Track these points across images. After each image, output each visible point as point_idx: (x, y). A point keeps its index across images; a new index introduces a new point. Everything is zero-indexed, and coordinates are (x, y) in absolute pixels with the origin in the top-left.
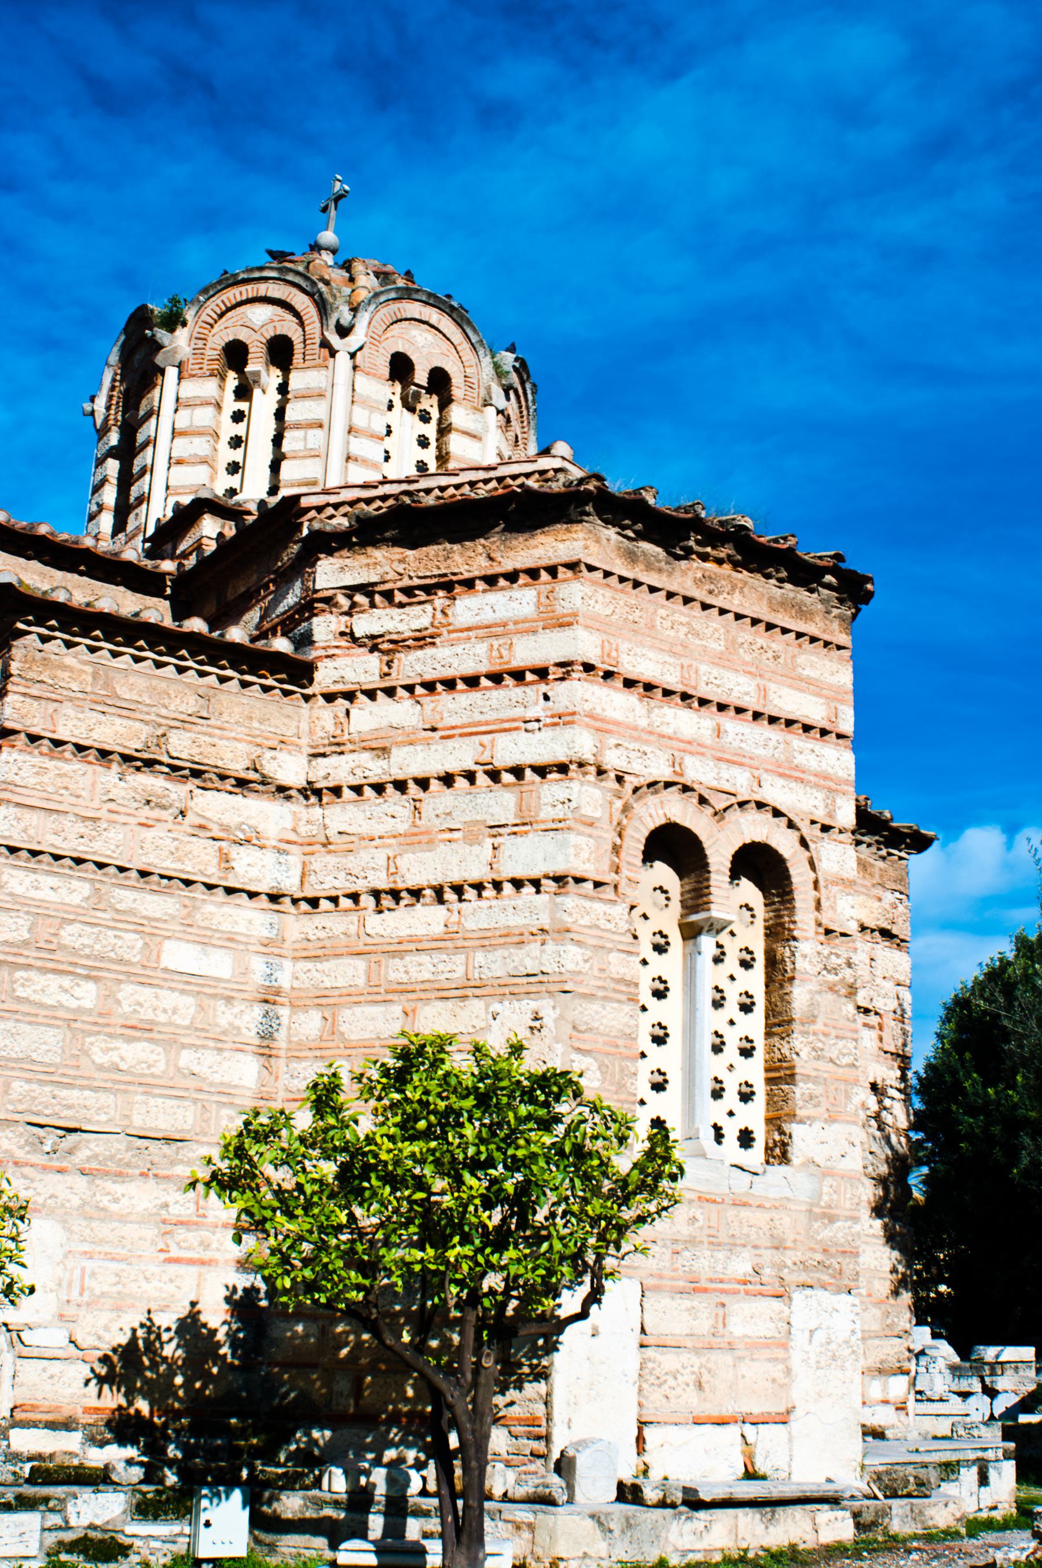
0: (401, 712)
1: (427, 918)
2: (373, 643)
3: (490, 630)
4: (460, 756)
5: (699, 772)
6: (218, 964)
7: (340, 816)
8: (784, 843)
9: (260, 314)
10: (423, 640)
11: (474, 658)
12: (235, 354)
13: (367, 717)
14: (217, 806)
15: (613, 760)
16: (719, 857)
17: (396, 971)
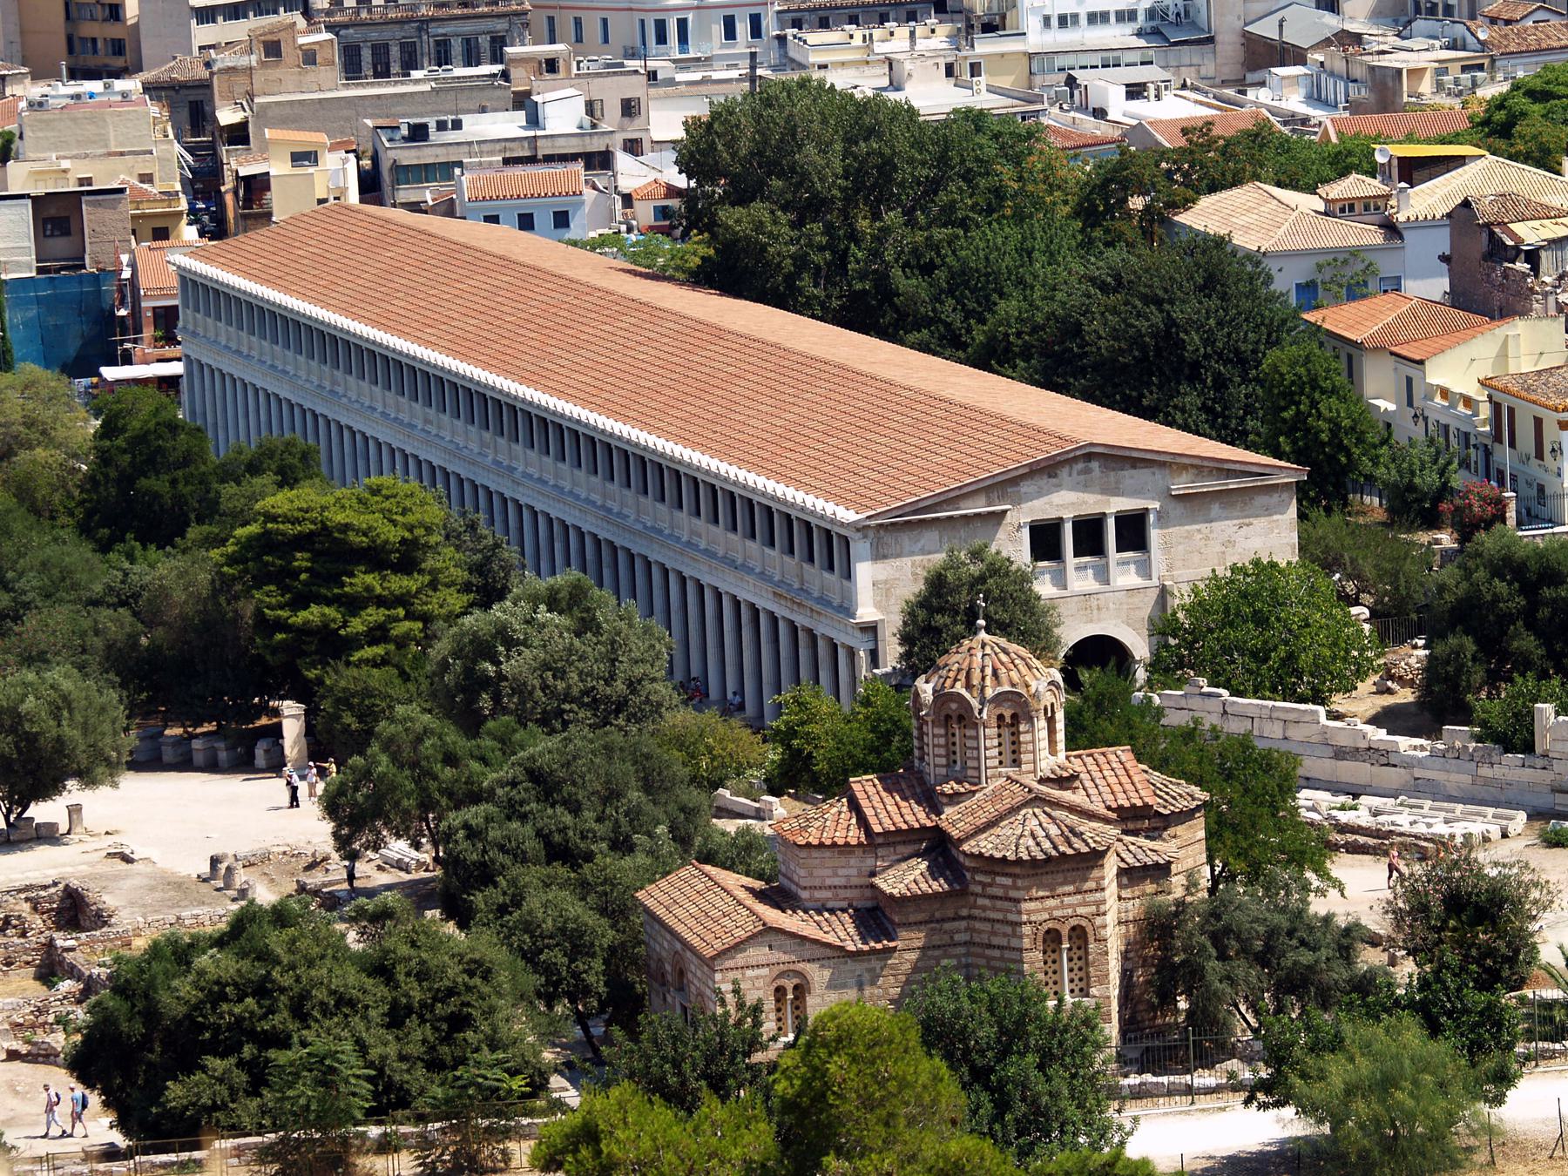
0: (987, 902)
1: (997, 953)
2: (980, 883)
3: (1003, 886)
4: (999, 916)
5: (1057, 913)
6: (954, 962)
7: (978, 925)
8: (1084, 923)
9: (954, 706)
10: (990, 885)
11: (1000, 892)
12: (948, 717)
13: (980, 901)
14: (947, 926)
15: (1033, 918)
16: (1065, 932)
17: (993, 963)
